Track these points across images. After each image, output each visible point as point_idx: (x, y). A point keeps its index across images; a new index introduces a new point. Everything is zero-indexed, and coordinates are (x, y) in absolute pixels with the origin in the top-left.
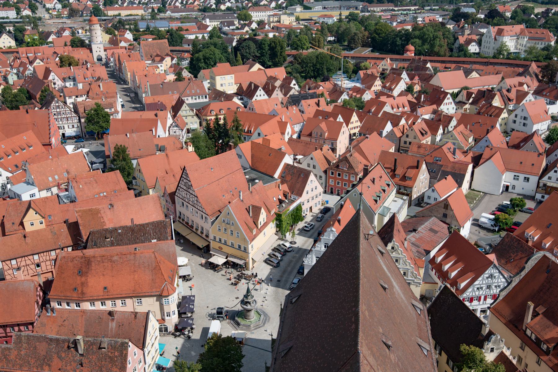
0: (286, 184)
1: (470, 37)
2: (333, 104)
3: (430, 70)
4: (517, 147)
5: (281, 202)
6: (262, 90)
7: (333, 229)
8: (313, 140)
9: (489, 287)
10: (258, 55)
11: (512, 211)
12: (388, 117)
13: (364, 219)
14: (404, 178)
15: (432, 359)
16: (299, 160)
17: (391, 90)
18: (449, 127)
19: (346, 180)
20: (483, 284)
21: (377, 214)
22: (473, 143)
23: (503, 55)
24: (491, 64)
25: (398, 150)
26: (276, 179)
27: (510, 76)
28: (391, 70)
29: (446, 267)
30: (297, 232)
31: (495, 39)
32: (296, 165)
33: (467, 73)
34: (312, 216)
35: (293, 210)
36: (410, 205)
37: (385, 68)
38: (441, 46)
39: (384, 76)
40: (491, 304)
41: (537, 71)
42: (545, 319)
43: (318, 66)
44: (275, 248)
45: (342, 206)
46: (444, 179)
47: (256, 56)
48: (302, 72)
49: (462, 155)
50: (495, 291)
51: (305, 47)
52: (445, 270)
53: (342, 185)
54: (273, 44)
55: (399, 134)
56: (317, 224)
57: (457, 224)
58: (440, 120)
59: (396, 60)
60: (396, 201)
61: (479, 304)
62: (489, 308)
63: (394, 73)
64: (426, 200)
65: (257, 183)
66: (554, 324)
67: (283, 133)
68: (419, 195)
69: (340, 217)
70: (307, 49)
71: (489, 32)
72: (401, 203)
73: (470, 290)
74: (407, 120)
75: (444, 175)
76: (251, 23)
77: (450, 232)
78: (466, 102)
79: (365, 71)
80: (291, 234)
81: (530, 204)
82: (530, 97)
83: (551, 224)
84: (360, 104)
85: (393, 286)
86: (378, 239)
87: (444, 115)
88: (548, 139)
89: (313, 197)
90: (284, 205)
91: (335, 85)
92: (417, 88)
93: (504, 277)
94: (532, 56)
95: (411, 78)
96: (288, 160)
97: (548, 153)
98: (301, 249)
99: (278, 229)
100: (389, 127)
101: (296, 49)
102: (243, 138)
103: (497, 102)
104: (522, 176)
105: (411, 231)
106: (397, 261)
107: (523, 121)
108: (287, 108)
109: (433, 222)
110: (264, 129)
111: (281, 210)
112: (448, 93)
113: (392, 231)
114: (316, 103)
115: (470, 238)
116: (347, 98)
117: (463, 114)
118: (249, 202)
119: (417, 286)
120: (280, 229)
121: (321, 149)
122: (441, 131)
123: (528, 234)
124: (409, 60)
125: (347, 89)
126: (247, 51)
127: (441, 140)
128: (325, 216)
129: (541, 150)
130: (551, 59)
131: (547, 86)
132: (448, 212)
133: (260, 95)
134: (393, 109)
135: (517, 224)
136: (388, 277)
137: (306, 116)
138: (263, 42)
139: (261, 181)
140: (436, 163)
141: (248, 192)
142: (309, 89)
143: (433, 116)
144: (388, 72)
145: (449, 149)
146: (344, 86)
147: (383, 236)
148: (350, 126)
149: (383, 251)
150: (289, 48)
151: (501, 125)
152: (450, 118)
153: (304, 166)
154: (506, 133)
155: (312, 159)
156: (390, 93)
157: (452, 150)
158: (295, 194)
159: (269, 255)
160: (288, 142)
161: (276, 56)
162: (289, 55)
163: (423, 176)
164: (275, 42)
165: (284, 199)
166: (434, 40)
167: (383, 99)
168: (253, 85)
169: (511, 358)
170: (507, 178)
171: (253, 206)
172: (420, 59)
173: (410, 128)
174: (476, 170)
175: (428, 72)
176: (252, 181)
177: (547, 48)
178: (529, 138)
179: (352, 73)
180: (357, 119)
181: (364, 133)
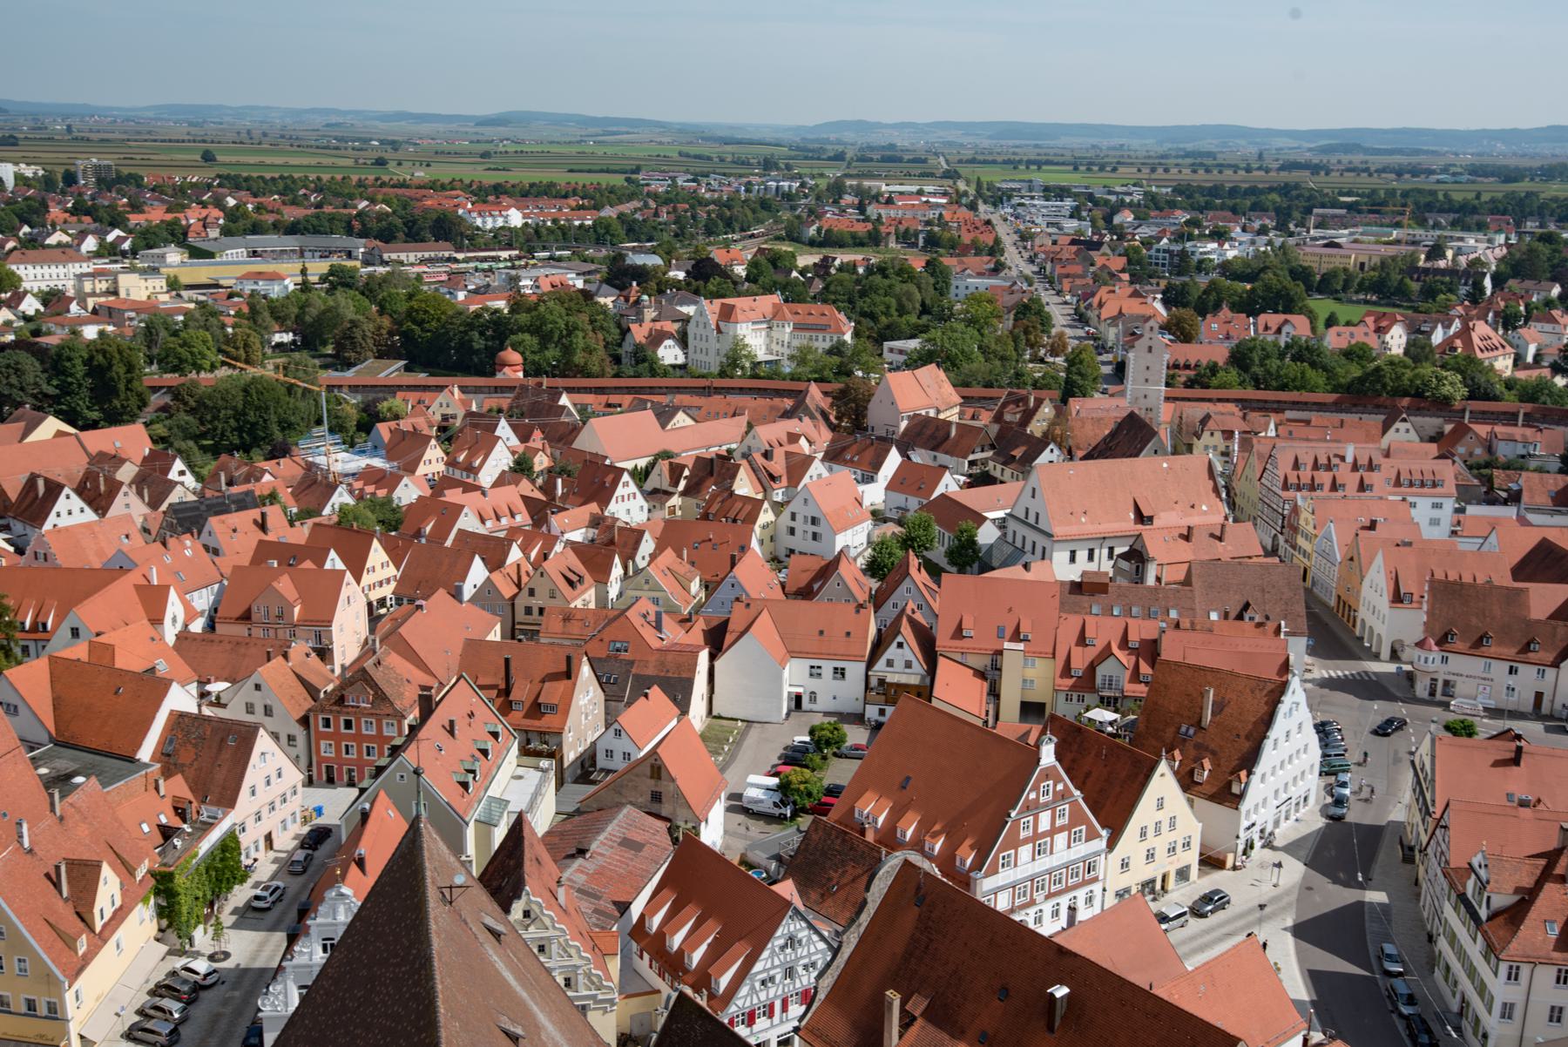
0: (179, 777)
1: (658, 326)
2: (310, 522)
3: (570, 414)
4: (806, 593)
5: (167, 833)
6: (73, 496)
7: (345, 890)
8: (258, 632)
9: (790, 972)
10: (51, 391)
11: (817, 758)
12: (472, 545)
13: (433, 845)
14: (536, 709)
16: (218, 698)
17: (473, 471)
18: (638, 558)
19: (370, 738)
20: (773, 967)
21: (472, 824)
22: (703, 595)
23: (743, 368)
24: (718, 390)
25: (511, 633)
26: (146, 766)
27: (766, 420)
28: (465, 416)
29: (677, 941)
30: (227, 919)
31: (719, 331)
32: (207, 711)
33: (664, 416)
34: (275, 861)
35: (211, 854)
36: (560, 783)
37: (449, 411)
38: (589, 351)
39: (448, 434)
40: (801, 1019)
41: (825, 403)
42: (931, 1029)
43: (252, 417)
44: (158, 986)
45: (365, 816)
46: (643, 699)
47: (46, 396)
48: (203, 436)
49: (677, 627)
50: (806, 980)
51: (207, 364)
52: (676, 947)
53: (360, 752)
54: (100, 358)
55: (508, 590)
56: (294, 884)
57: (690, 816)
58: (611, 542)
59: (477, 390)
60: (520, 777)
61: (772, 1026)
62: (796, 1030)
63: (476, 426)
64: (602, 761)
65: (78, 785)
66: (953, 1036)
67: (157, 621)
68: (581, 749)
69: (362, 850)
70: (213, 368)
71: (701, 313)
72: (536, 781)
73: (744, 990)
74: (525, 549)
75: (642, 687)
76: (19, 297)
77: (675, 841)
78: (671, 489)
79: (392, 424)
80: (211, 930)
81: (856, 736)
82: (817, 468)
83: (908, 779)
84: (389, 516)
85: (537, 1027)
86: (481, 896)
87: (620, 529)
88: (874, 568)
89: (274, 802)
90: (177, 842)
91: (310, 467)
92: (541, 462)
93: (823, 938)
94: (808, 369)
95: (524, 437)
96: (181, 699)
97: (878, 600)
98: (246, 971)
99: (165, 923)
100: (478, 573)
101: (175, 369)
102: (17, 651)
103: (744, 485)
104: (827, 667)
105: (572, 856)
106: (542, 949)
107: (811, 529)
108: (164, 544)
109: (628, 820)
110: (89, 614)
111: (169, 859)
112: (623, 470)
113: (520, 864)
114: (255, 522)
115: (726, 846)
116: (349, 500)
117: (667, 522)
118: (56, 851)
119: (605, 1011)
120: (172, 920)
121: (285, 656)
122: (617, 571)
123: (861, 814)
124: (511, 389)
125: (346, 475)
126: (14, 380)
127: (620, 595)
128: (317, 854)
129: (862, 597)
130: (849, 374)
131: (851, 439)
132: (663, 786)
133: (69, 511)
134: (483, 521)
135: (834, 791)
136: (521, 1003)
137: (226, 563)
138: (67, 353)
139: (93, 779)
140: (616, 657)
141: (49, 820)
142: (230, 483)
143: (592, 533)
144: (458, 423)
145: (645, 616)
146: (338, 468)
147: (495, 884)
148: (367, 579)
149: (500, 928)
150: (155, 367)
151: (761, 542)
152: (636, 535)
153: (234, 712)
154: (776, 561)
155: (258, 687)
156: (470, 480)
157: (652, 618)
158: (211, 803)
159: (140, 1012)
160: (176, 647)
161: (116, 393)
162: (155, 389)
163: (587, 695)
164: (104, 353)
165: (176, 822)
166: (569, 334)
167: (453, 496)
168: (41, 483)
170: (794, 676)
171: (71, 864)
172: (540, 384)
173: (535, 569)
174: (717, 664)
175: (564, 419)
176: (61, 781)
177: (837, 350)
178: (829, 569)
179: (359, 429)
180: (385, 558)
181: (410, 594)
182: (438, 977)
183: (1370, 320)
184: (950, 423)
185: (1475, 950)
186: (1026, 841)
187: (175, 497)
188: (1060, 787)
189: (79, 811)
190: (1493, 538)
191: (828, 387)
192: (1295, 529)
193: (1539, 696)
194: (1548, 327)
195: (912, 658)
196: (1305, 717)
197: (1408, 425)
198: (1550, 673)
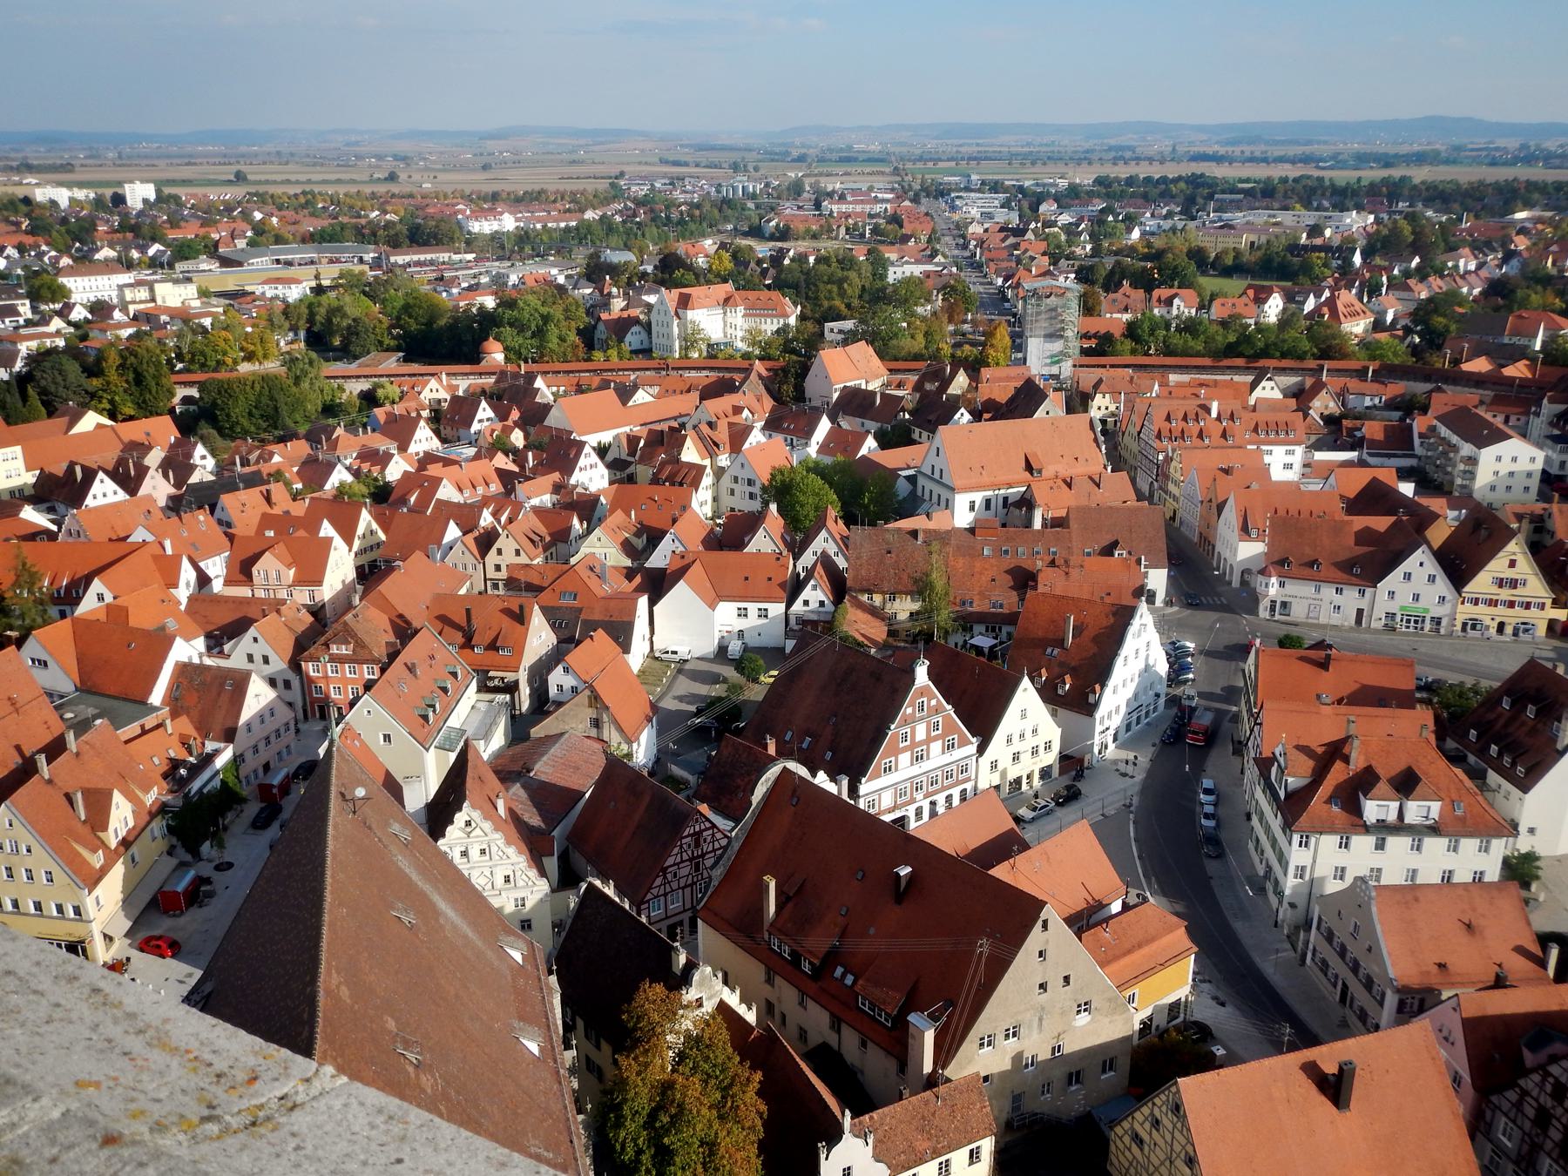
3: (544, 396)
6: (107, 480)
12: (449, 510)
15: (555, 1061)
26: (156, 709)
32: (208, 661)
71: (661, 302)
74: (496, 514)
76: (69, 307)
82: (756, 437)
95: (502, 415)
96: (188, 650)
103: (690, 453)
112: (582, 444)
121: (278, 611)
133: (104, 492)
134: (461, 490)
136: (423, 894)
143: (555, 497)
158: (214, 739)
167: (434, 470)
168: (78, 469)
169: (742, 1010)
182: (329, 873)
183: (1251, 293)
184: (873, 393)
185: (1276, 823)
186: (905, 749)
187: (194, 479)
188: (933, 702)
189: (92, 747)
190: (1332, 479)
191: (770, 364)
192: (1167, 477)
193: (1360, 612)
194: (1405, 295)
195: (823, 598)
196: (1152, 635)
197: (1272, 383)
198: (1369, 591)
